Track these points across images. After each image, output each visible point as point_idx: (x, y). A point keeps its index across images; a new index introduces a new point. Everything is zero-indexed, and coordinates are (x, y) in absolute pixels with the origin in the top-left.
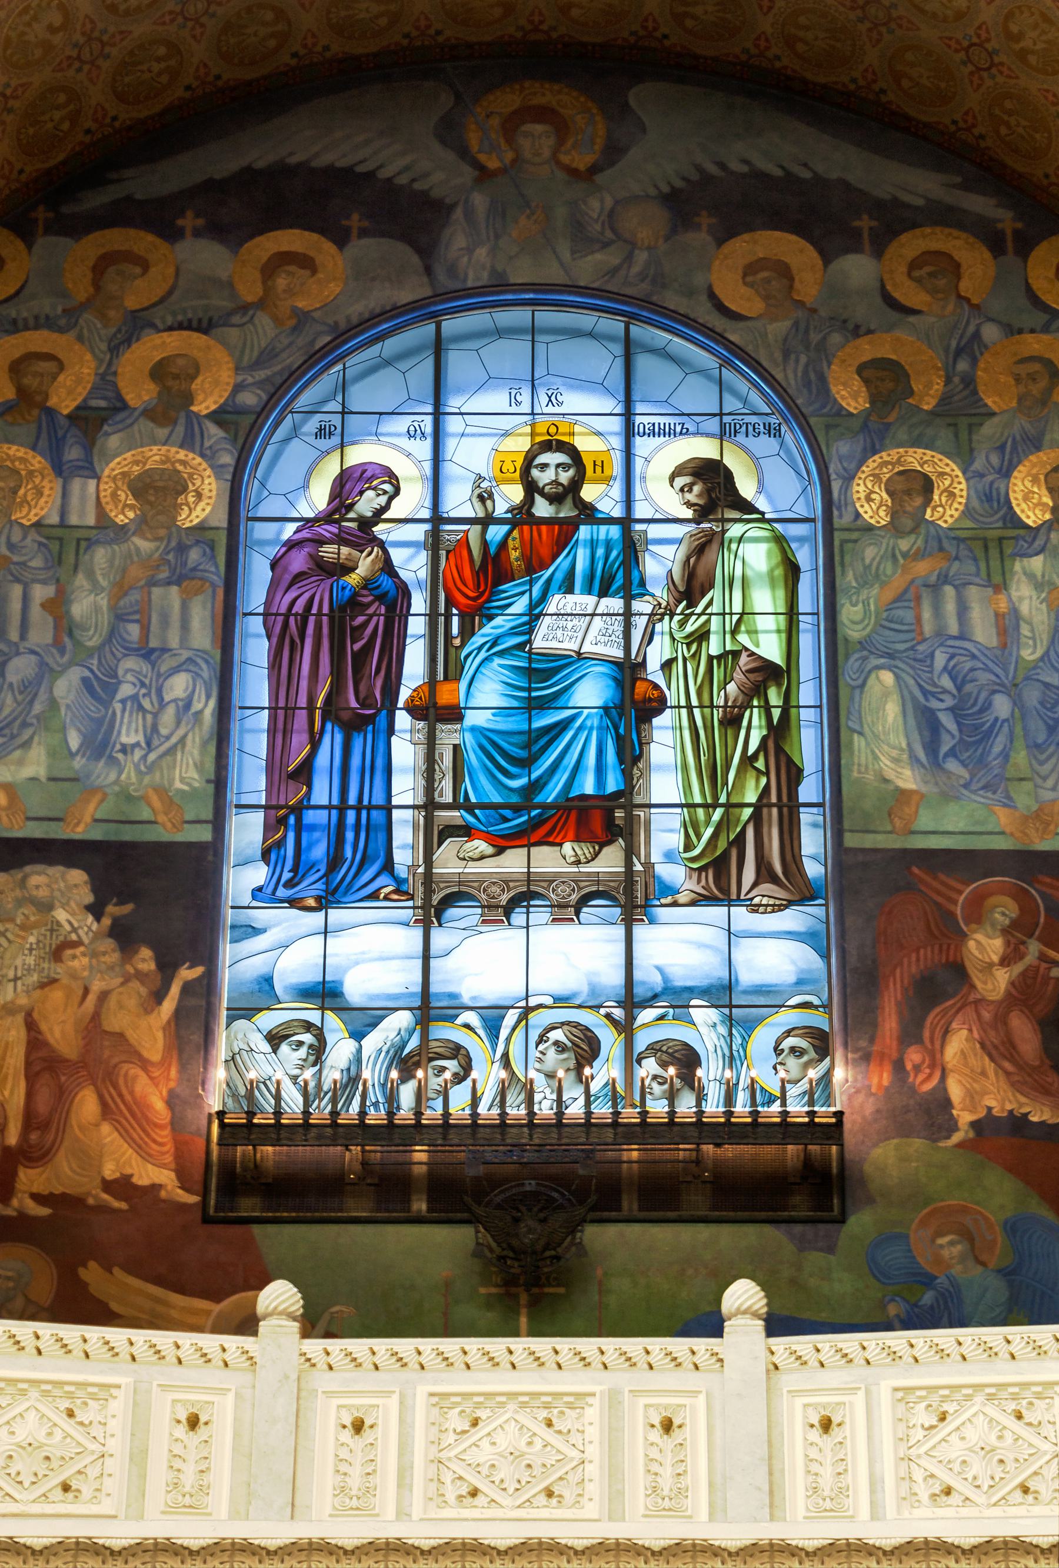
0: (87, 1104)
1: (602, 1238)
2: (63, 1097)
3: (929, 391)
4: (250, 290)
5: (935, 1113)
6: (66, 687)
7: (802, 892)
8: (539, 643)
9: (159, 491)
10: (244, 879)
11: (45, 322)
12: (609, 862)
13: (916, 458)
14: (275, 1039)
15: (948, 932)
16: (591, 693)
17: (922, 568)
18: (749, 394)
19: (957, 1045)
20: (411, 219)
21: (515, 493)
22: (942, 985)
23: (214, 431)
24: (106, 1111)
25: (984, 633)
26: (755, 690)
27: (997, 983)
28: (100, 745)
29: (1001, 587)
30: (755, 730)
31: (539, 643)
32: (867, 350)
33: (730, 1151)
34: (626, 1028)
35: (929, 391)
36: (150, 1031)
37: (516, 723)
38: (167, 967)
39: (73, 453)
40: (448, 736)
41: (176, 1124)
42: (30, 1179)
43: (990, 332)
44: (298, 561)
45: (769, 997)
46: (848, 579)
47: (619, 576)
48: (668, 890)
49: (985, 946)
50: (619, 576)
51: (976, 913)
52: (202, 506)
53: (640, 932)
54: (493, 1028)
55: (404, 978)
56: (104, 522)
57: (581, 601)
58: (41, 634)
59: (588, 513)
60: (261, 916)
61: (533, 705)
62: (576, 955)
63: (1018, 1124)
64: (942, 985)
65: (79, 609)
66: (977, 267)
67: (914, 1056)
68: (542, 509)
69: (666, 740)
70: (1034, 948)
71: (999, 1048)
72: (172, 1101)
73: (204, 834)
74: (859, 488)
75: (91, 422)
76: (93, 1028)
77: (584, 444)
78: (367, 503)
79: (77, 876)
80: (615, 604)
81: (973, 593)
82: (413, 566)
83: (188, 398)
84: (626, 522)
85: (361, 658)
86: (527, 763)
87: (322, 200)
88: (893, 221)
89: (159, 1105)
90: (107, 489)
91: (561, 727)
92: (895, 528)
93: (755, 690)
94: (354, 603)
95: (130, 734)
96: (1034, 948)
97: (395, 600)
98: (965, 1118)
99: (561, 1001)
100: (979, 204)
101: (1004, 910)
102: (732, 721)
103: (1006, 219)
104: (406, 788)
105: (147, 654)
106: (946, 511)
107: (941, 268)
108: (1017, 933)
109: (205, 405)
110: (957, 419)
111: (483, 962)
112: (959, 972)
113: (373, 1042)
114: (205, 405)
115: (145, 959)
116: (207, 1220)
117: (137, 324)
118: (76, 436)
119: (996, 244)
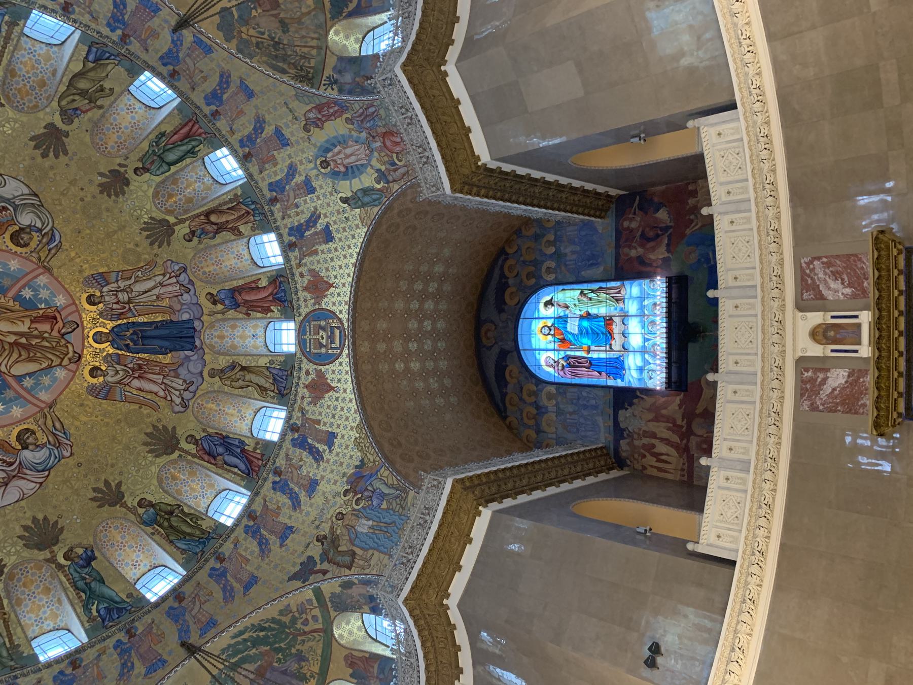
0: (664, 412)
1: (691, 319)
2: (663, 416)
3: (532, 269)
4: (515, 381)
5: (666, 260)
6: (585, 413)
7: (624, 285)
8: (576, 332)
9: (550, 397)
10: (619, 383)
11: (521, 415)
12: (617, 320)
13: (543, 270)
14: (651, 378)
15: (630, 260)
16: (586, 324)
17: (563, 268)
18: (533, 299)
19: (652, 257)
20: (503, 355)
21: (550, 337)
22: (641, 260)
23: (540, 387)
24: (666, 408)
25: (575, 257)
26: (585, 295)
27: (640, 251)
28: (595, 407)
29: (566, 254)
30: (592, 295)
31: (576, 332)
32: (525, 280)
33: (673, 296)
34: (648, 316)
35: (532, 269)
36: (649, 400)
37: (590, 336)
38: (637, 397)
39: (543, 410)
40: (593, 348)
41: (668, 396)
42: (679, 422)
43: (522, 259)
44: (562, 373)
45: (642, 290)
46: (565, 281)
47: (564, 319)
48: (622, 309)
49: (633, 253)
50: (564, 319)
51: (627, 255)
52: (552, 389)
53: (630, 314)
54: (649, 340)
55: (638, 357)
56: (556, 405)
57: (569, 326)
58: (576, 417)
59: (553, 325)
60: (626, 380)
61: (587, 333)
62: (634, 326)
63: (668, 245)
64: (641, 260)
65: (571, 410)
66: (510, 262)
67: (655, 264)
68: (552, 332)
69: (593, 311)
70: (634, 244)
71: (653, 249)
72: (663, 397)
73: (612, 390)
74: (549, 279)
75: (538, 407)
76: (649, 410)
77: (541, 326)
78: (552, 362)
79: (620, 412)
80: (569, 320)
81: (568, 258)
82: (562, 354)
83: (534, 391)
84: (554, 318)
85: (579, 363)
86: (598, 334)
87: (501, 370)
88: (503, 276)
89: (664, 399)
90: (550, 405)
91: (592, 329)
92: (556, 273)
93: (585, 295)
94: (569, 364)
95: (593, 402)
96: (634, 244)
97: (567, 358)
98: (666, 255)
99: (643, 328)
100: (500, 262)
101: (626, 250)
102: (590, 299)
103: (503, 257)
104: (603, 355)
105: (579, 399)
106: (553, 264)
107: (511, 268)
108: (630, 247)
109: (535, 388)
110: (536, 263)
111: (635, 341)
112: (638, 257)
113: (651, 361)
114: (535, 388)
115: (635, 401)
116: (686, 390)
117: (521, 399)
118: (540, 410)
119: (507, 259)
